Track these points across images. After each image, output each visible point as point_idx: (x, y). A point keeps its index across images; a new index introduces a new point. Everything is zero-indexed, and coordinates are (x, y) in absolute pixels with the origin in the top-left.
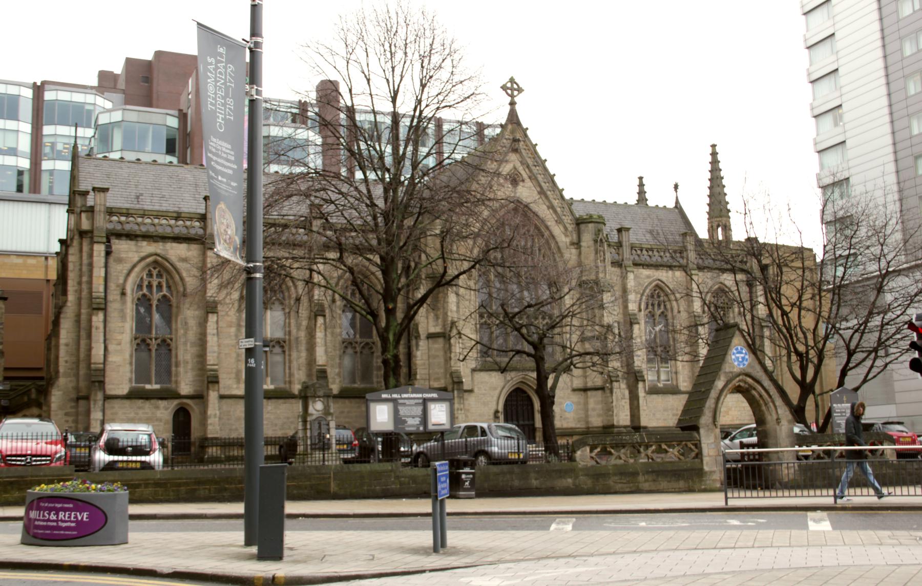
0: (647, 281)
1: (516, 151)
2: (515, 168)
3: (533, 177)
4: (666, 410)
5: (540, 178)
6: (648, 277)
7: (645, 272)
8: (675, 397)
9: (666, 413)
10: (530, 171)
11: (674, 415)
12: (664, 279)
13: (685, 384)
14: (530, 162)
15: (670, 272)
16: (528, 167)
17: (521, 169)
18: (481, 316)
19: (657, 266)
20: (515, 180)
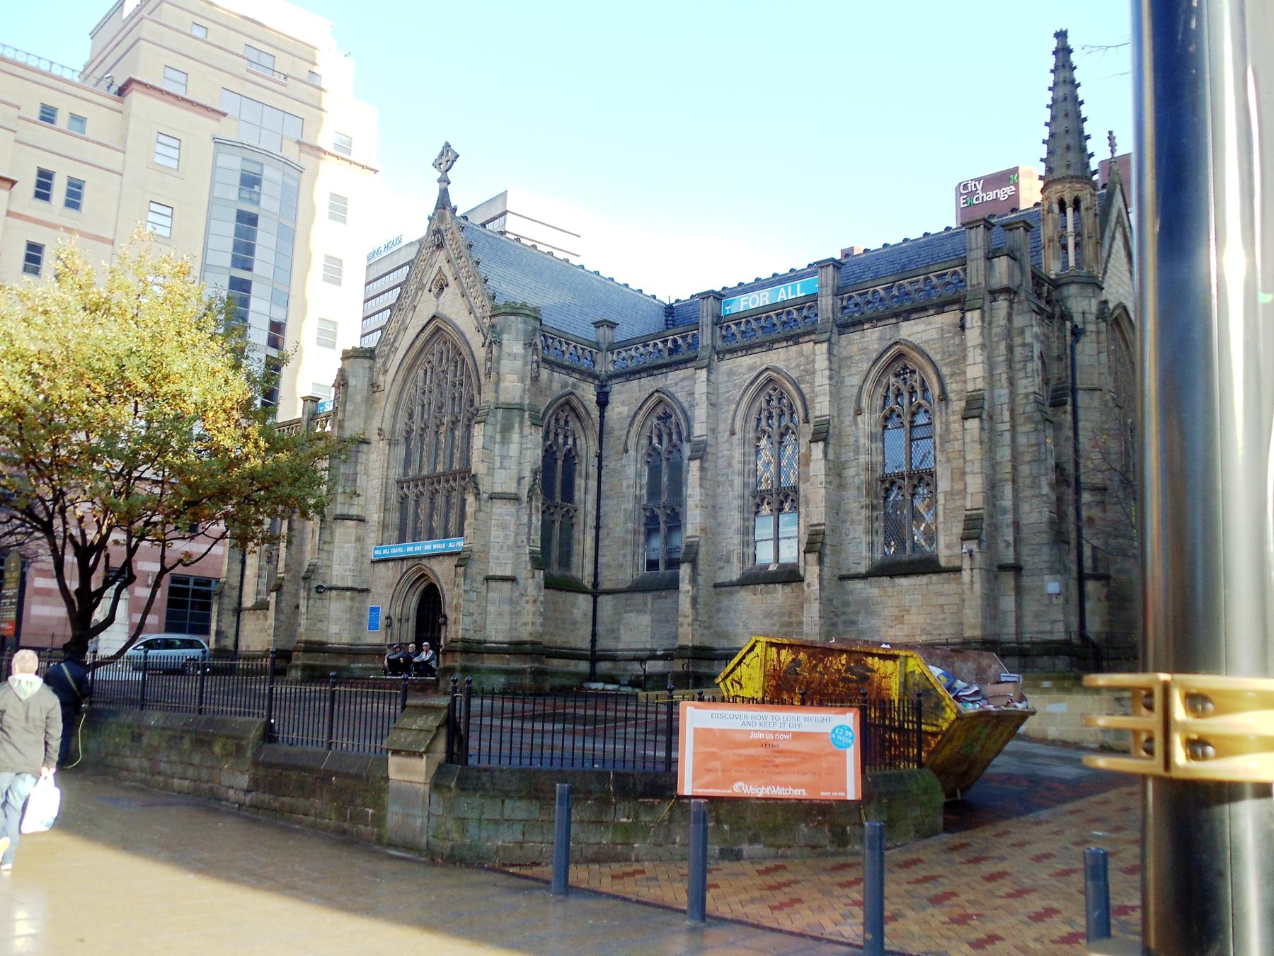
1: (440, 246)
2: (440, 270)
4: (768, 615)
6: (751, 369)
9: (768, 622)
11: (782, 625)
12: (781, 365)
15: (794, 348)
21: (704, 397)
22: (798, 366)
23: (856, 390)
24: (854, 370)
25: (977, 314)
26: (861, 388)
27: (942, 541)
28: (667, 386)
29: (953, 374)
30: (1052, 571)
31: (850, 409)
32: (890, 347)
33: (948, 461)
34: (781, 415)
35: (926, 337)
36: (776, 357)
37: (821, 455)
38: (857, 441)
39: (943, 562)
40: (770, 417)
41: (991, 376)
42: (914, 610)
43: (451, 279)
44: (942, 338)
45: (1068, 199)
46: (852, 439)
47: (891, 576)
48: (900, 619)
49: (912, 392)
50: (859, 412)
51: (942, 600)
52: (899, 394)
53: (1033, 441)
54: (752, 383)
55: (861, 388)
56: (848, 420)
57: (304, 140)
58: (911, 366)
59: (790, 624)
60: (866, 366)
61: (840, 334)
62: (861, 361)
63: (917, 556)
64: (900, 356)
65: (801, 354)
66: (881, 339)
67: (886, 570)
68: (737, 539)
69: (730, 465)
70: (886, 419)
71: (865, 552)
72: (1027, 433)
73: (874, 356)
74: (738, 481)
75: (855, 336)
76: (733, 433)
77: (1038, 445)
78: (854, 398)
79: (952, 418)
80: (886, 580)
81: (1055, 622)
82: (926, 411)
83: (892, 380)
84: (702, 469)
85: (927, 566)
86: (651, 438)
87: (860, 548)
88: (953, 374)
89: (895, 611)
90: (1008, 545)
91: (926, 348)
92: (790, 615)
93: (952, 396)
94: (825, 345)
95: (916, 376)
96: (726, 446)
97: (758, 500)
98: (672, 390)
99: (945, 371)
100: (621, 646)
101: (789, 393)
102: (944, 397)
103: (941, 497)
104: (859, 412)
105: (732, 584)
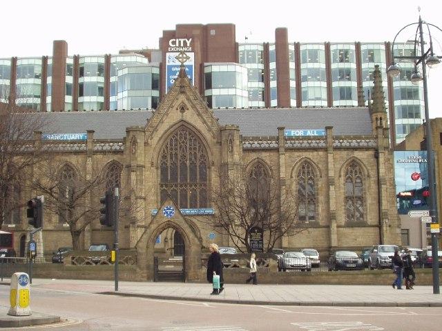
1: (183, 92)
3: (194, 107)
6: (299, 156)
7: (297, 154)
14: (192, 98)
17: (186, 102)
18: (162, 186)
20: (183, 109)
26: (341, 169)
27: (369, 217)
31: (338, 175)
34: (308, 172)
40: (304, 173)
43: (189, 106)
47: (352, 227)
52: (351, 172)
54: (300, 161)
55: (341, 169)
56: (336, 178)
60: (343, 162)
64: (353, 160)
65: (318, 154)
66: (348, 155)
67: (349, 225)
75: (339, 152)
76: (292, 177)
80: (351, 229)
82: (361, 179)
86: (251, 174)
87: (342, 219)
91: (362, 160)
102: (368, 176)
103: (368, 205)
104: (340, 176)
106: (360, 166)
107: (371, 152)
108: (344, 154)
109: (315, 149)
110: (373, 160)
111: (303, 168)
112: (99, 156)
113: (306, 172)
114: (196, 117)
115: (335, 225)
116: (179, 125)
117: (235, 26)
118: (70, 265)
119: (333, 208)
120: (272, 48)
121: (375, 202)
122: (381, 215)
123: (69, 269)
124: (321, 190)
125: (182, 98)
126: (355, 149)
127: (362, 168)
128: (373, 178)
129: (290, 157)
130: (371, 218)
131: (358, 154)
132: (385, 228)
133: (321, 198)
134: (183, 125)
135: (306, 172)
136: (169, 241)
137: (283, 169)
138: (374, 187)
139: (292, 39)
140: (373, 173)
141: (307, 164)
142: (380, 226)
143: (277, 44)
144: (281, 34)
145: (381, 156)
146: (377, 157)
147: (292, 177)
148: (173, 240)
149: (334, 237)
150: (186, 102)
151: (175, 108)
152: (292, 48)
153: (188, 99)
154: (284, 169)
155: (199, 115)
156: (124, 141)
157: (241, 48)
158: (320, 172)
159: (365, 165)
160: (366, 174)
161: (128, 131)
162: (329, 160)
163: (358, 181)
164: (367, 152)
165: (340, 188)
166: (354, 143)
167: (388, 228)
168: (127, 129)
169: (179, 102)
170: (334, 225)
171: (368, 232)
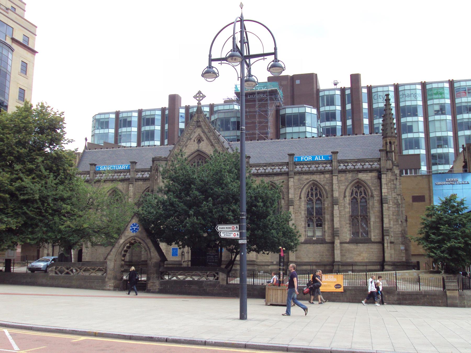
0: (306, 182)
1: (199, 126)
2: (199, 135)
3: (208, 139)
4: (315, 252)
5: (211, 138)
6: (307, 179)
7: (305, 177)
8: (322, 245)
10: (207, 135)
11: (320, 255)
12: (318, 180)
13: (329, 238)
14: (206, 131)
15: (322, 175)
16: (206, 134)
17: (202, 135)
19: (312, 173)
20: (200, 140)
21: (292, 187)
22: (324, 181)
23: (344, 190)
24: (343, 184)
25: (385, 175)
26: (346, 190)
27: (372, 234)
28: (274, 181)
29: (375, 190)
30: (402, 244)
32: (355, 180)
33: (374, 213)
34: (316, 195)
35: (366, 178)
36: (315, 177)
37: (337, 209)
38: (345, 205)
39: (373, 240)
40: (312, 195)
41: (388, 193)
42: (364, 253)
43: (204, 138)
44: (372, 179)
45: (392, 142)
46: (343, 204)
47: (357, 243)
48: (359, 255)
49: (361, 192)
50: (345, 197)
51: (372, 250)
52: (356, 192)
53: (396, 210)
54: (308, 183)
55: (346, 190)
56: (341, 198)
57: (14, 37)
58: (360, 185)
59: (323, 255)
60: (347, 184)
61: (339, 173)
62: (345, 182)
63: (363, 238)
64: (358, 182)
65: (325, 177)
66: (352, 177)
67: (353, 241)
68: (303, 230)
69: (300, 207)
70: (352, 199)
71: (348, 236)
72: (395, 208)
73: (350, 181)
74: (303, 212)
75: (344, 175)
76: (300, 198)
77: (398, 211)
78: (343, 193)
79: (375, 202)
80: (355, 245)
81: (403, 257)
83: (354, 188)
84: (294, 209)
85: (368, 241)
87: (346, 234)
88: (375, 190)
89: (358, 253)
90: (392, 237)
91: (367, 181)
92: (323, 252)
93: (375, 195)
94: (336, 177)
95: (362, 189)
96: (298, 202)
97: (308, 219)
98: (276, 182)
99: (373, 188)
100: (258, 261)
101: (320, 188)
102: (372, 196)
103: (372, 223)
104: (345, 197)
105: (302, 243)
106: (364, 186)
107: (375, 174)
108: (349, 176)
109: (322, 172)
110: (376, 181)
111: (312, 189)
112: (141, 183)
113: (314, 193)
114: (210, 147)
115: (338, 241)
116: (196, 154)
117: (316, 75)
118: (54, 274)
119: (336, 225)
120: (348, 92)
121: (378, 220)
122: (383, 232)
123: (52, 278)
124: (328, 209)
125: (198, 131)
126: (359, 171)
127: (366, 189)
128: (377, 198)
129: (299, 180)
130: (375, 235)
131: (362, 176)
132: (386, 245)
133: (327, 217)
134: (199, 155)
135: (314, 193)
136: (186, 255)
137: (291, 191)
138: (377, 205)
139: (364, 82)
140: (376, 193)
141: (315, 186)
142: (382, 242)
143: (351, 89)
144: (355, 79)
145: (383, 176)
146: (380, 178)
147: (300, 198)
148: (190, 254)
149: (337, 252)
150: (202, 135)
151: (192, 140)
152: (365, 91)
153: (204, 132)
154: (292, 191)
155: (212, 145)
156: (150, 170)
157: (321, 94)
158: (327, 194)
159: (368, 186)
160: (370, 194)
161: (154, 160)
162: (334, 182)
163: (363, 200)
164: (370, 174)
165: (345, 207)
166: (359, 166)
167: (389, 244)
168: (153, 159)
169: (196, 134)
170: (337, 242)
171: (372, 249)
